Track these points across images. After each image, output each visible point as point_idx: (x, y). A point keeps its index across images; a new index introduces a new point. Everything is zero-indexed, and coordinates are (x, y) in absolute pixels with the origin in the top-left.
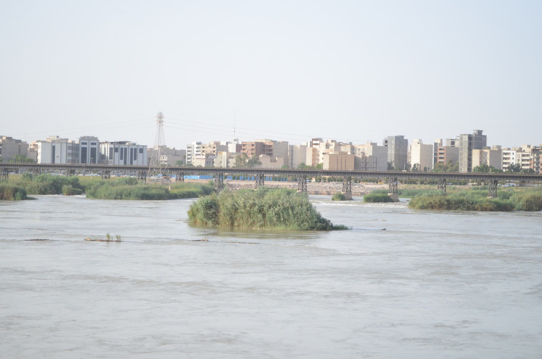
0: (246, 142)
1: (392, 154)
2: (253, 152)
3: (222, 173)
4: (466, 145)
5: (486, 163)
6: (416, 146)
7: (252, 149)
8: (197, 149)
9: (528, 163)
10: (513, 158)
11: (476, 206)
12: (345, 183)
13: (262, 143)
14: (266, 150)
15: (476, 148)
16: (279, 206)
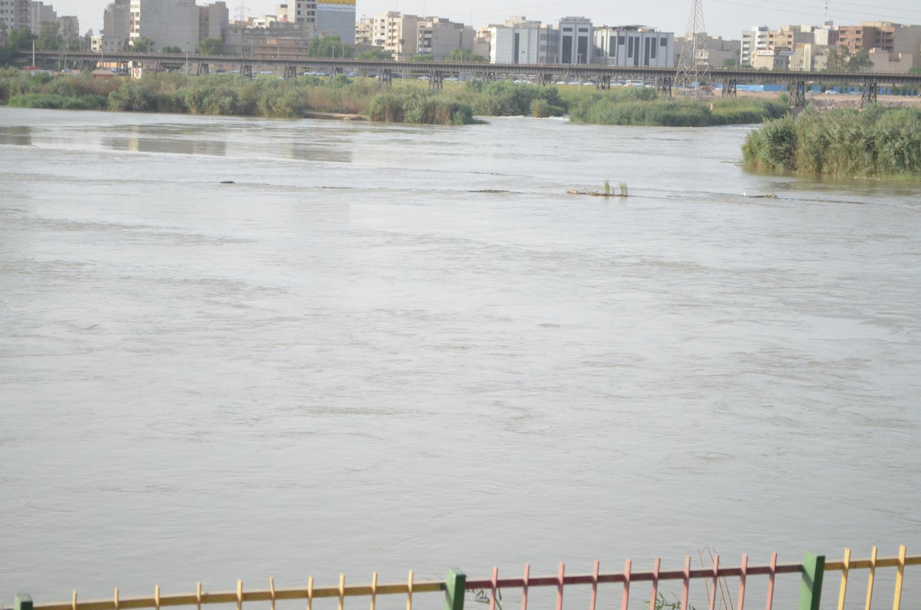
0: (847, 27)
2: (858, 44)
7: (857, 39)
8: (760, 39)
14: (881, 41)
16: (902, 139)
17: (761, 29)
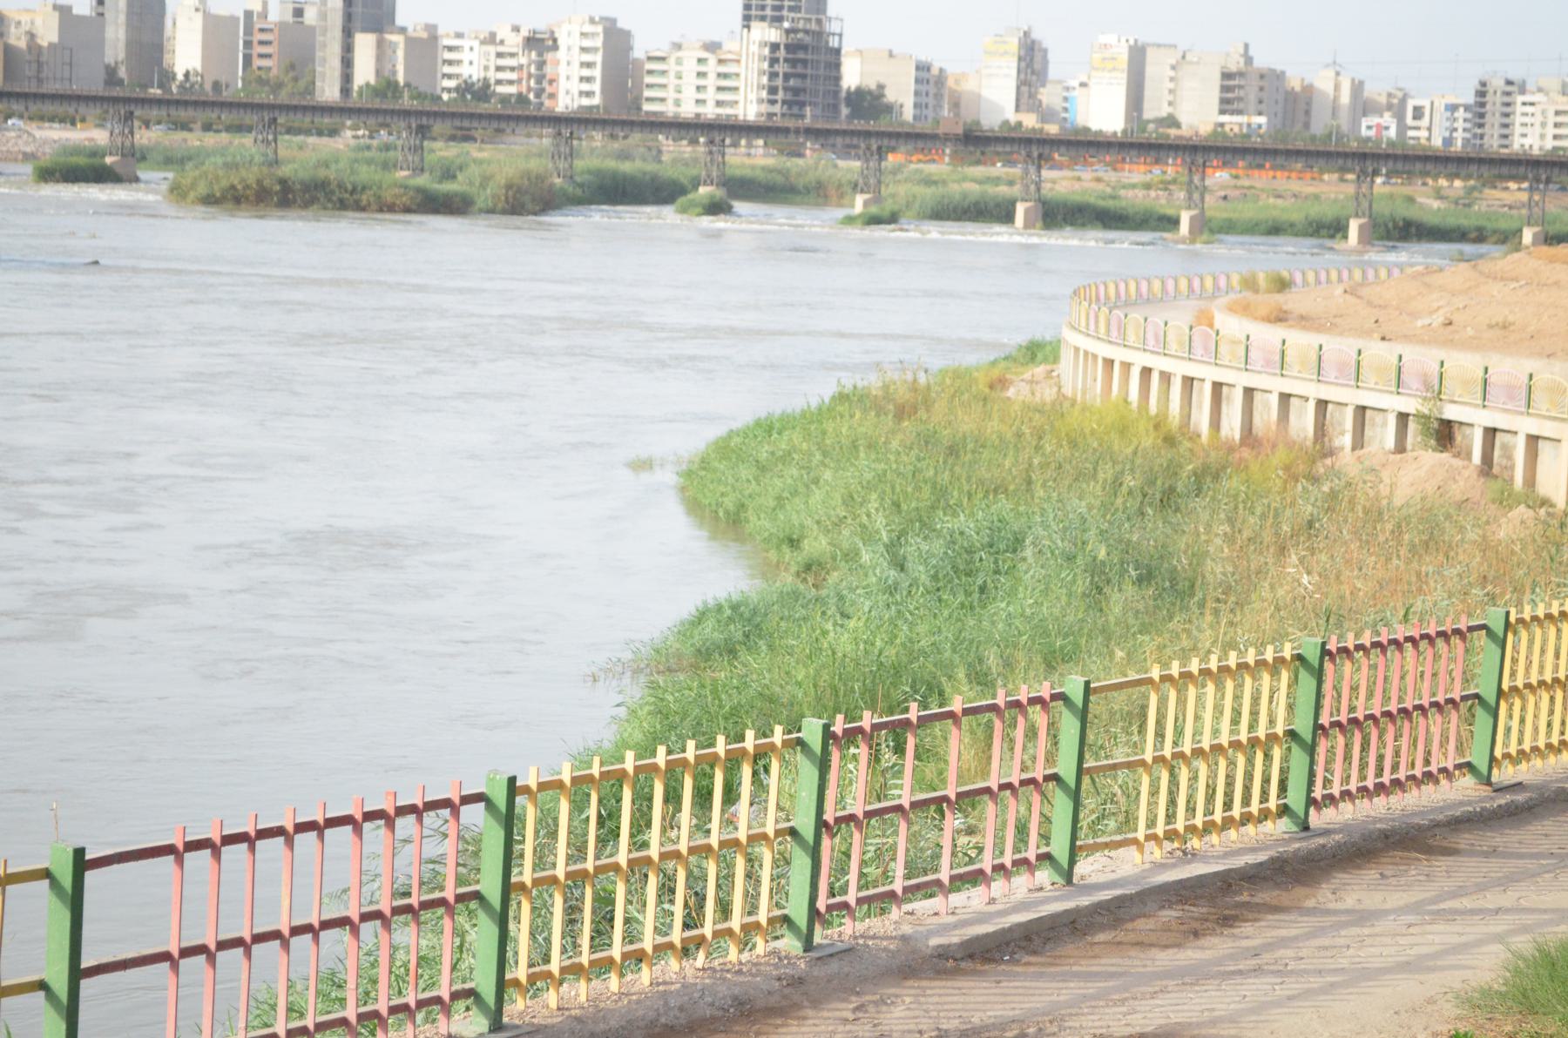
1: (118, 39)
4: (336, 20)
5: (394, 73)
6: (190, 19)
9: (513, 76)
10: (471, 63)
11: (364, 197)
15: (365, 30)
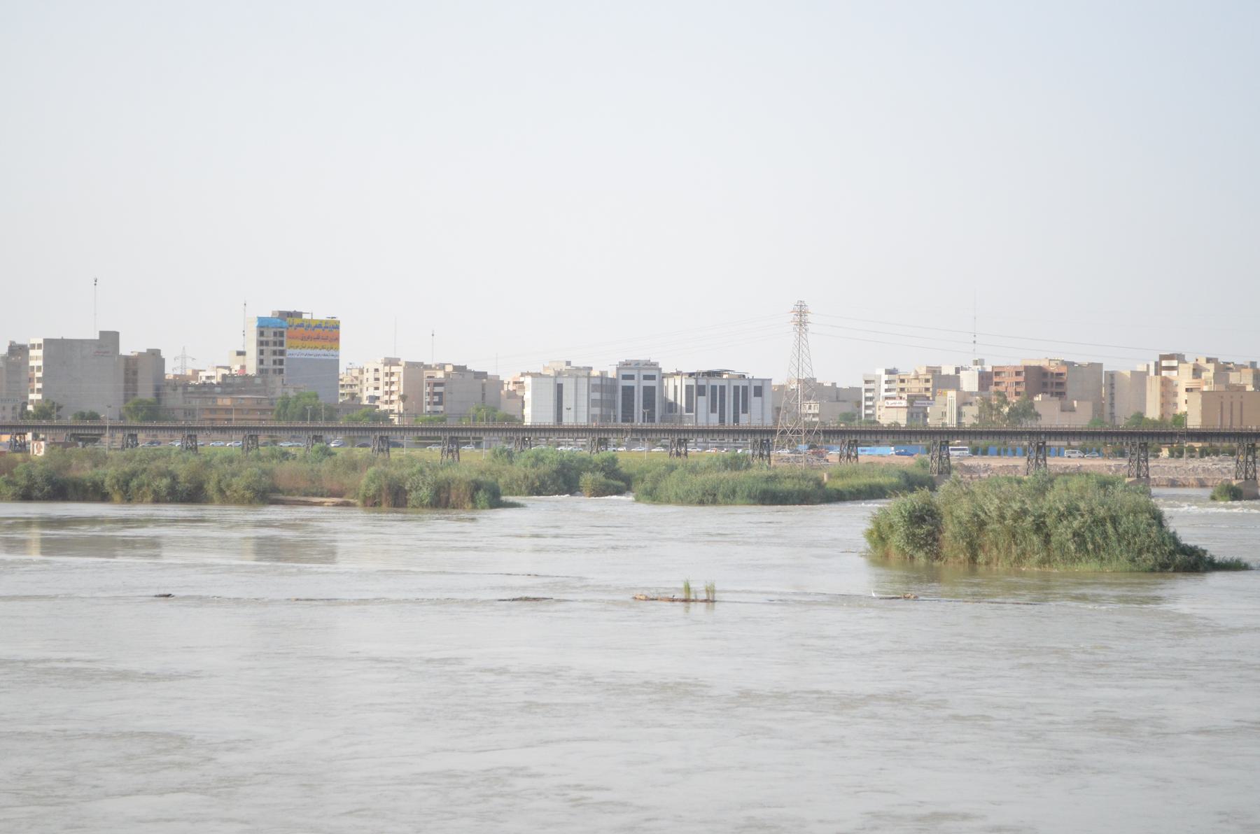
2: (1018, 390)
3: (946, 439)
7: (1017, 383)
12: (1241, 458)
13: (1040, 368)
14: (1049, 385)
16: (1082, 516)
17: (889, 372)
